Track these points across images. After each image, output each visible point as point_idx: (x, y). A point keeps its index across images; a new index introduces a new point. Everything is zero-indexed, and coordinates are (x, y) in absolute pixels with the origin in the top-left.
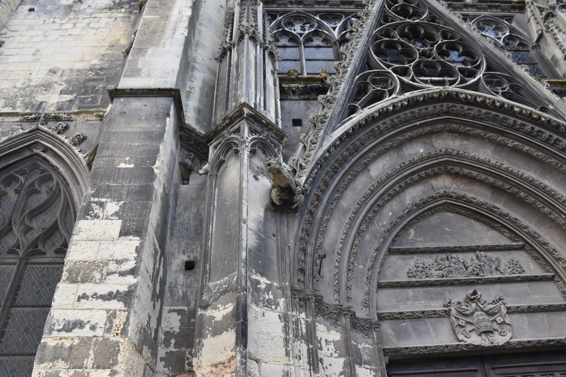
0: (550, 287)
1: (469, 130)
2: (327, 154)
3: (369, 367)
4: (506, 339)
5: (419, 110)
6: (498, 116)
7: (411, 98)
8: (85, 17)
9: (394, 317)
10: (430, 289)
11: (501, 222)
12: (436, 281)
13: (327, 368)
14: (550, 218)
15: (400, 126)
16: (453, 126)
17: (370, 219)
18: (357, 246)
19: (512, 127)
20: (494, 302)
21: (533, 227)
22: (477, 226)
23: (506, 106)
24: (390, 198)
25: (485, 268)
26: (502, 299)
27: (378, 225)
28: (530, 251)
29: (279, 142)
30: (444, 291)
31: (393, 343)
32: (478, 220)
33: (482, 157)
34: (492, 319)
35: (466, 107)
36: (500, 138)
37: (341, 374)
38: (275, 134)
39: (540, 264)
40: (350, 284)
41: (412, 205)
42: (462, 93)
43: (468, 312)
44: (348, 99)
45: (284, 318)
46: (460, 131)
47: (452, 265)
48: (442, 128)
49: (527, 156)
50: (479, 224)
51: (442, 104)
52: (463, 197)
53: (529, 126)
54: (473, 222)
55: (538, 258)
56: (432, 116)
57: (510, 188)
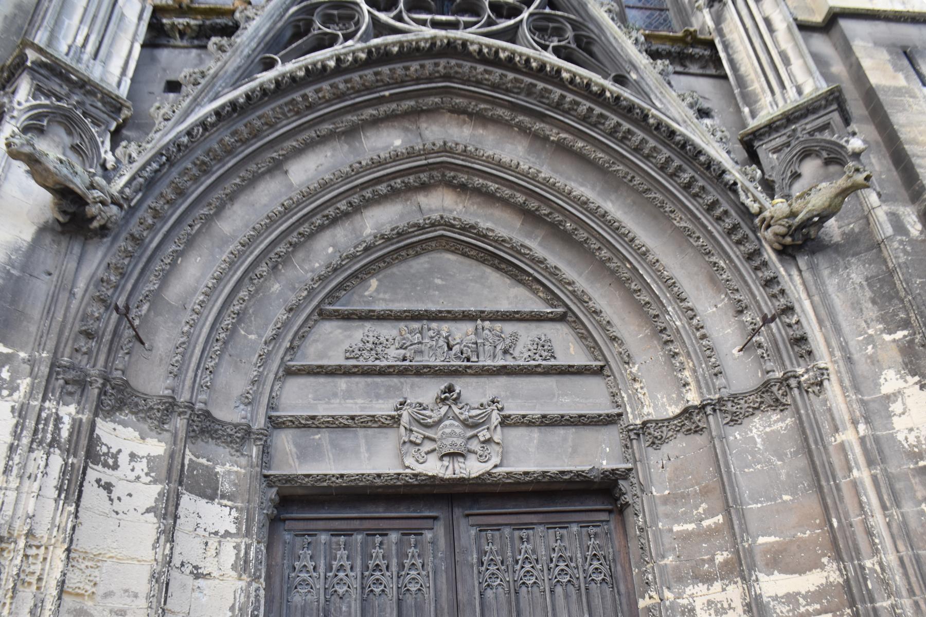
0: (594, 384)
1: (486, 110)
2: (185, 139)
3: (229, 503)
4: (488, 466)
6: (535, 86)
9: (300, 423)
10: (379, 380)
11: (531, 271)
12: (389, 367)
13: (119, 499)
14: (609, 268)
16: (457, 101)
17: (280, 256)
18: (244, 301)
19: (558, 106)
20: (482, 405)
21: (582, 283)
22: (494, 277)
26: (498, 402)
27: (302, 268)
28: (573, 325)
29: (109, 115)
30: (402, 383)
31: (291, 466)
32: (498, 269)
33: (506, 158)
34: (470, 433)
35: (481, 68)
36: (538, 126)
37: (148, 511)
38: (102, 100)
39: (587, 346)
40: (212, 364)
41: (375, 237)
42: (472, 43)
43: (429, 420)
44: (262, 45)
45: (21, 412)
46: (470, 110)
48: (436, 103)
49: (580, 157)
50: (498, 275)
51: (437, 61)
52: (472, 227)
53: (585, 105)
54: (488, 270)
55: (585, 336)
56: (418, 80)
57: (550, 213)
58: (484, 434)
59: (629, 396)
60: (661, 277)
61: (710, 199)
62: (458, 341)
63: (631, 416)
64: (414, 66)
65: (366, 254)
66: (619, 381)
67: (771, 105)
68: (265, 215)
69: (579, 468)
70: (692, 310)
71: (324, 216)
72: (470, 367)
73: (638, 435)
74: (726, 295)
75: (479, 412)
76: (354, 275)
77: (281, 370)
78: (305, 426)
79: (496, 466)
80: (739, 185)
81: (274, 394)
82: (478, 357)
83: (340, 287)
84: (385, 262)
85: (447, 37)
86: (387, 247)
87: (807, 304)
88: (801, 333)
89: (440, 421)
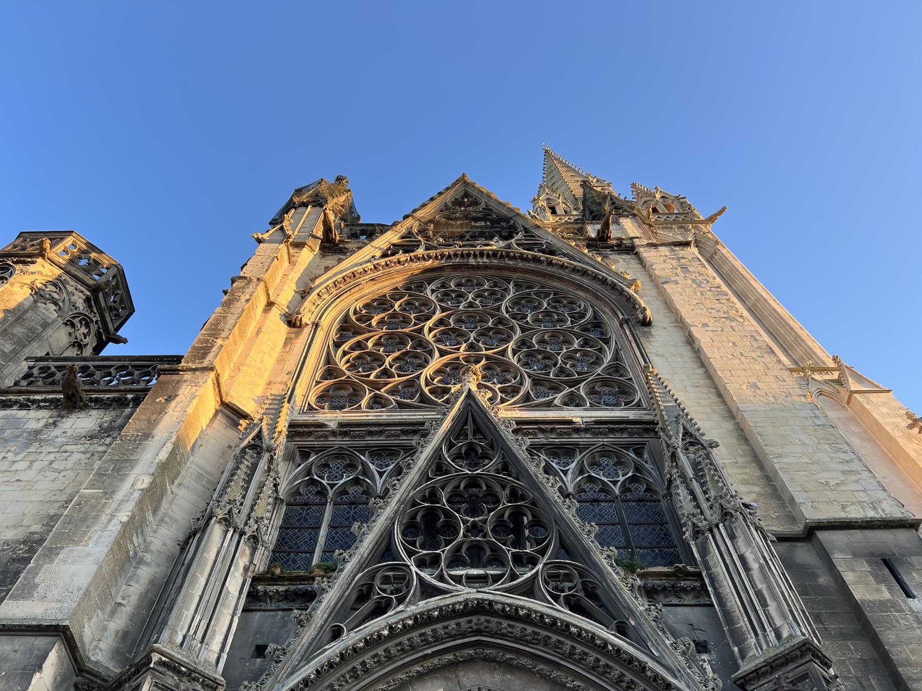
1: (511, 659)
5: (432, 631)
6: (550, 638)
7: (419, 613)
8: (52, 450)
15: (402, 657)
16: (488, 652)
23: (559, 624)
35: (505, 623)
36: (555, 674)
42: (497, 603)
44: (333, 615)
46: (498, 659)
48: (471, 655)
51: (469, 618)
53: (593, 656)
56: (454, 637)
64: (452, 624)
67: (756, 648)
85: (476, 599)
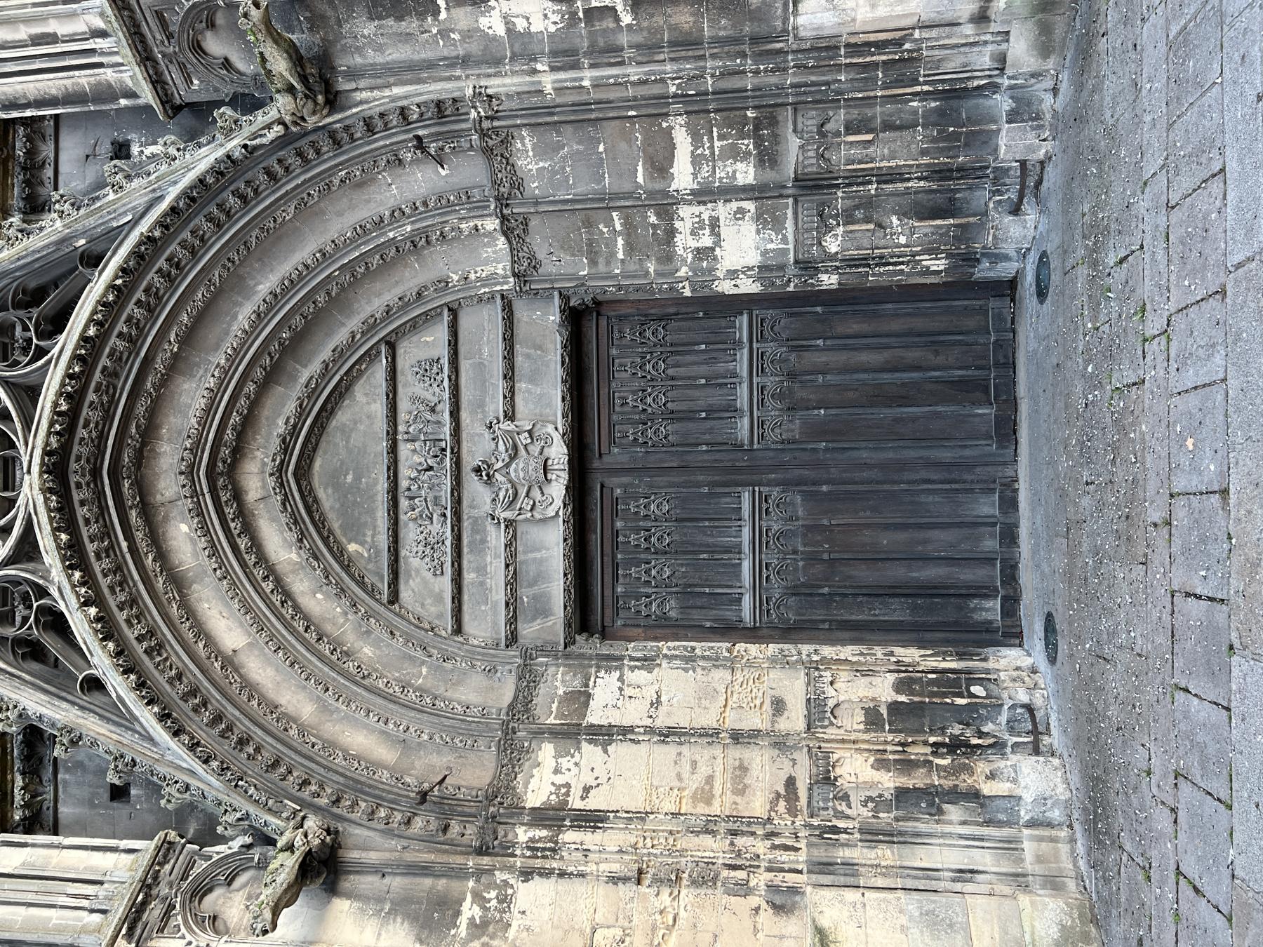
1: (138, 427)
2: (215, 764)
3: (592, 679)
4: (557, 437)
5: (92, 541)
6: (105, 368)
7: (63, 562)
11: (337, 378)
12: (453, 530)
13: (597, 778)
15: (131, 585)
16: (127, 460)
17: (335, 650)
19: (133, 341)
21: (354, 323)
22: (342, 417)
23: (83, 352)
24: (290, 604)
25: (431, 433)
26: (491, 423)
28: (400, 335)
32: (332, 412)
33: (202, 403)
34: (522, 451)
35: (81, 433)
36: (159, 366)
37: (606, 751)
40: (459, 707)
41: (301, 548)
42: (47, 444)
43: (510, 492)
45: (527, 875)
46: (138, 445)
47: (423, 493)
48: (131, 484)
49: (200, 319)
50: (340, 413)
51: (73, 486)
52: (284, 441)
54: (334, 423)
55: (415, 325)
56: (103, 509)
57: (269, 354)
58: (524, 439)
59: (483, 286)
60: (352, 240)
61: (263, 177)
62: (423, 460)
63: (505, 287)
64: (82, 512)
65: (321, 557)
66: (467, 294)
67: (121, 72)
68: (289, 669)
69: (559, 346)
70: (393, 212)
71: (283, 606)
72: (452, 449)
73: (526, 282)
74: (379, 173)
75: (501, 442)
76: (346, 569)
77: (456, 639)
78: (515, 611)
79: (556, 429)
80: (249, 143)
81: (483, 644)
82: (442, 440)
83: (361, 583)
84: (329, 537)
85: (41, 475)
86: (311, 535)
87: (397, 91)
88: (432, 106)
89: (510, 481)
